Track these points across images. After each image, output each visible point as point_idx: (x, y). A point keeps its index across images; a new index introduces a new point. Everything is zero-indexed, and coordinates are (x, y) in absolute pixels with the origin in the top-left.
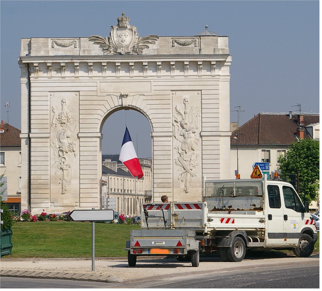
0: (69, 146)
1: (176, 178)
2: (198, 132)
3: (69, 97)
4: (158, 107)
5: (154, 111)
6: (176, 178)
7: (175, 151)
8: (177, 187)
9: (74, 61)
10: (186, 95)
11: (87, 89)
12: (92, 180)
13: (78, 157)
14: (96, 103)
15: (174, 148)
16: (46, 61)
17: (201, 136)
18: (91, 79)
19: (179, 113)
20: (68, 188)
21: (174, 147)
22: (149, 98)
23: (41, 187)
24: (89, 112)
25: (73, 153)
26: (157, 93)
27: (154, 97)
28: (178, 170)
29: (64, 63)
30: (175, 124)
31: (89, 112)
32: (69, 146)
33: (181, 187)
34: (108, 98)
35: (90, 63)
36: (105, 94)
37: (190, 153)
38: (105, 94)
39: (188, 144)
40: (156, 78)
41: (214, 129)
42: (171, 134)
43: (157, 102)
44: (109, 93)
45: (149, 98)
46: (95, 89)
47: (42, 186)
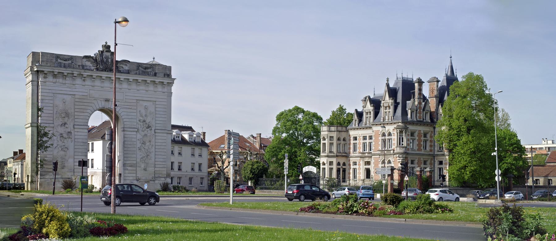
0: (68, 134)
1: (138, 160)
2: (153, 129)
3: (68, 98)
4: (129, 110)
5: (125, 113)
6: (138, 160)
7: (138, 142)
9: (74, 72)
10: (145, 104)
11: (81, 94)
13: (73, 142)
14: (86, 104)
16: (54, 71)
17: (155, 132)
18: (84, 87)
19: (141, 116)
20: (66, 165)
22: (123, 104)
24: (82, 110)
25: (70, 139)
27: (126, 104)
28: (140, 155)
29: (66, 73)
30: (139, 123)
31: (82, 110)
32: (68, 134)
33: (142, 167)
34: (95, 102)
35: (85, 75)
36: (93, 99)
37: (148, 144)
38: (93, 99)
40: (127, 90)
41: (163, 128)
42: (136, 130)
45: (123, 104)
46: (86, 94)
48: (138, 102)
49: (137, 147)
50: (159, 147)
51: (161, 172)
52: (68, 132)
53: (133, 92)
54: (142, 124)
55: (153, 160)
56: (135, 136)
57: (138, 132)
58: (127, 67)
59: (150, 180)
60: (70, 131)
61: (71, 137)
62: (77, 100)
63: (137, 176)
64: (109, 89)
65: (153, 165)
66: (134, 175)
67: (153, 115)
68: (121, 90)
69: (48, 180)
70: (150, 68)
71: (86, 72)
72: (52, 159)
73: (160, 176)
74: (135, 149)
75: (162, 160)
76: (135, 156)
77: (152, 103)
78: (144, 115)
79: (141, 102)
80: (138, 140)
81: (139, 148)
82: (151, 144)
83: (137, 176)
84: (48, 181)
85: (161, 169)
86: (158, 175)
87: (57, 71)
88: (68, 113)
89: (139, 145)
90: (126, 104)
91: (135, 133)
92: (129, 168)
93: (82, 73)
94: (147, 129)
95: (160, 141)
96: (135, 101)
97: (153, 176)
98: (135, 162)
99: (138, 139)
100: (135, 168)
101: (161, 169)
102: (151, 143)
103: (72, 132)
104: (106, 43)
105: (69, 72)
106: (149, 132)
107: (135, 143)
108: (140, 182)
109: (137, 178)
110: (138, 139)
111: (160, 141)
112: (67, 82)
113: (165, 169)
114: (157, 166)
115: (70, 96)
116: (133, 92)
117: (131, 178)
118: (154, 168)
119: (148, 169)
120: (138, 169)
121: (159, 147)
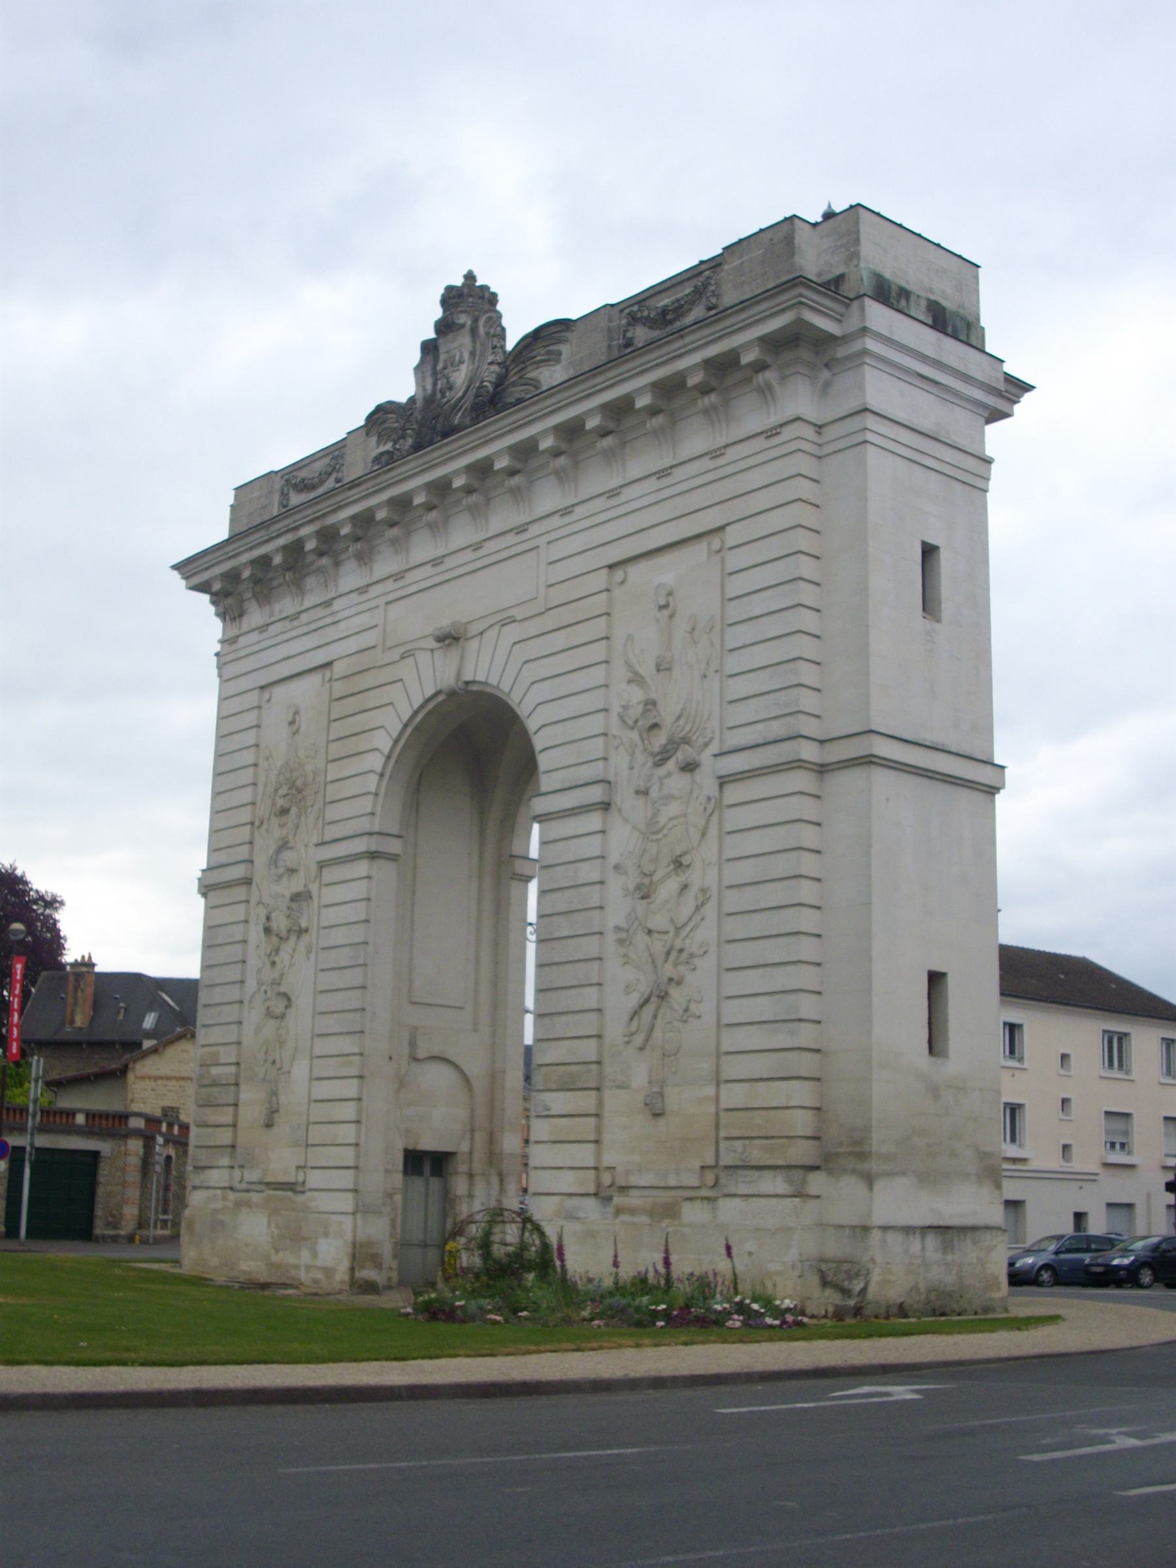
1: (615, 1030)
6: (615, 1030)
8: (619, 1087)
11: (351, 645)
18: (364, 597)
22: (533, 627)
26: (559, 595)
27: (548, 621)
29: (277, 550)
34: (405, 670)
35: (343, 522)
37: (668, 888)
38: (396, 654)
39: (660, 836)
42: (595, 794)
43: (559, 640)
44: (408, 647)
45: (533, 627)
48: (619, 575)
49: (611, 924)
51: (758, 1118)
52: (296, 897)
54: (634, 735)
55: (709, 1020)
56: (592, 846)
57: (613, 811)
58: (558, 367)
59: (687, 1199)
60: (301, 888)
61: (304, 924)
62: (339, 689)
64: (469, 555)
65: (706, 1066)
66: (584, 1155)
67: (712, 644)
68: (527, 535)
71: (340, 508)
72: (233, 1069)
73: (756, 1155)
74: (590, 947)
75: (765, 1008)
76: (590, 997)
77: (700, 550)
78: (646, 669)
79: (634, 571)
80: (617, 867)
81: (618, 929)
82: (685, 887)
83: (608, 1159)
86: (739, 1144)
87: (245, 558)
88: (299, 783)
89: (618, 910)
91: (593, 821)
92: (558, 1102)
94: (662, 771)
96: (599, 580)
97: (710, 1161)
98: (589, 1050)
99: (614, 857)
100: (587, 1101)
102: (695, 877)
103: (314, 888)
104: (470, 277)
105: (282, 541)
106: (678, 783)
107: (593, 896)
108: (618, 1211)
109: (606, 1179)
110: (614, 857)
112: (310, 601)
113: (801, 1093)
116: (587, 523)
117: (567, 1182)
118: (710, 1091)
119: (675, 1098)
120: (613, 1100)
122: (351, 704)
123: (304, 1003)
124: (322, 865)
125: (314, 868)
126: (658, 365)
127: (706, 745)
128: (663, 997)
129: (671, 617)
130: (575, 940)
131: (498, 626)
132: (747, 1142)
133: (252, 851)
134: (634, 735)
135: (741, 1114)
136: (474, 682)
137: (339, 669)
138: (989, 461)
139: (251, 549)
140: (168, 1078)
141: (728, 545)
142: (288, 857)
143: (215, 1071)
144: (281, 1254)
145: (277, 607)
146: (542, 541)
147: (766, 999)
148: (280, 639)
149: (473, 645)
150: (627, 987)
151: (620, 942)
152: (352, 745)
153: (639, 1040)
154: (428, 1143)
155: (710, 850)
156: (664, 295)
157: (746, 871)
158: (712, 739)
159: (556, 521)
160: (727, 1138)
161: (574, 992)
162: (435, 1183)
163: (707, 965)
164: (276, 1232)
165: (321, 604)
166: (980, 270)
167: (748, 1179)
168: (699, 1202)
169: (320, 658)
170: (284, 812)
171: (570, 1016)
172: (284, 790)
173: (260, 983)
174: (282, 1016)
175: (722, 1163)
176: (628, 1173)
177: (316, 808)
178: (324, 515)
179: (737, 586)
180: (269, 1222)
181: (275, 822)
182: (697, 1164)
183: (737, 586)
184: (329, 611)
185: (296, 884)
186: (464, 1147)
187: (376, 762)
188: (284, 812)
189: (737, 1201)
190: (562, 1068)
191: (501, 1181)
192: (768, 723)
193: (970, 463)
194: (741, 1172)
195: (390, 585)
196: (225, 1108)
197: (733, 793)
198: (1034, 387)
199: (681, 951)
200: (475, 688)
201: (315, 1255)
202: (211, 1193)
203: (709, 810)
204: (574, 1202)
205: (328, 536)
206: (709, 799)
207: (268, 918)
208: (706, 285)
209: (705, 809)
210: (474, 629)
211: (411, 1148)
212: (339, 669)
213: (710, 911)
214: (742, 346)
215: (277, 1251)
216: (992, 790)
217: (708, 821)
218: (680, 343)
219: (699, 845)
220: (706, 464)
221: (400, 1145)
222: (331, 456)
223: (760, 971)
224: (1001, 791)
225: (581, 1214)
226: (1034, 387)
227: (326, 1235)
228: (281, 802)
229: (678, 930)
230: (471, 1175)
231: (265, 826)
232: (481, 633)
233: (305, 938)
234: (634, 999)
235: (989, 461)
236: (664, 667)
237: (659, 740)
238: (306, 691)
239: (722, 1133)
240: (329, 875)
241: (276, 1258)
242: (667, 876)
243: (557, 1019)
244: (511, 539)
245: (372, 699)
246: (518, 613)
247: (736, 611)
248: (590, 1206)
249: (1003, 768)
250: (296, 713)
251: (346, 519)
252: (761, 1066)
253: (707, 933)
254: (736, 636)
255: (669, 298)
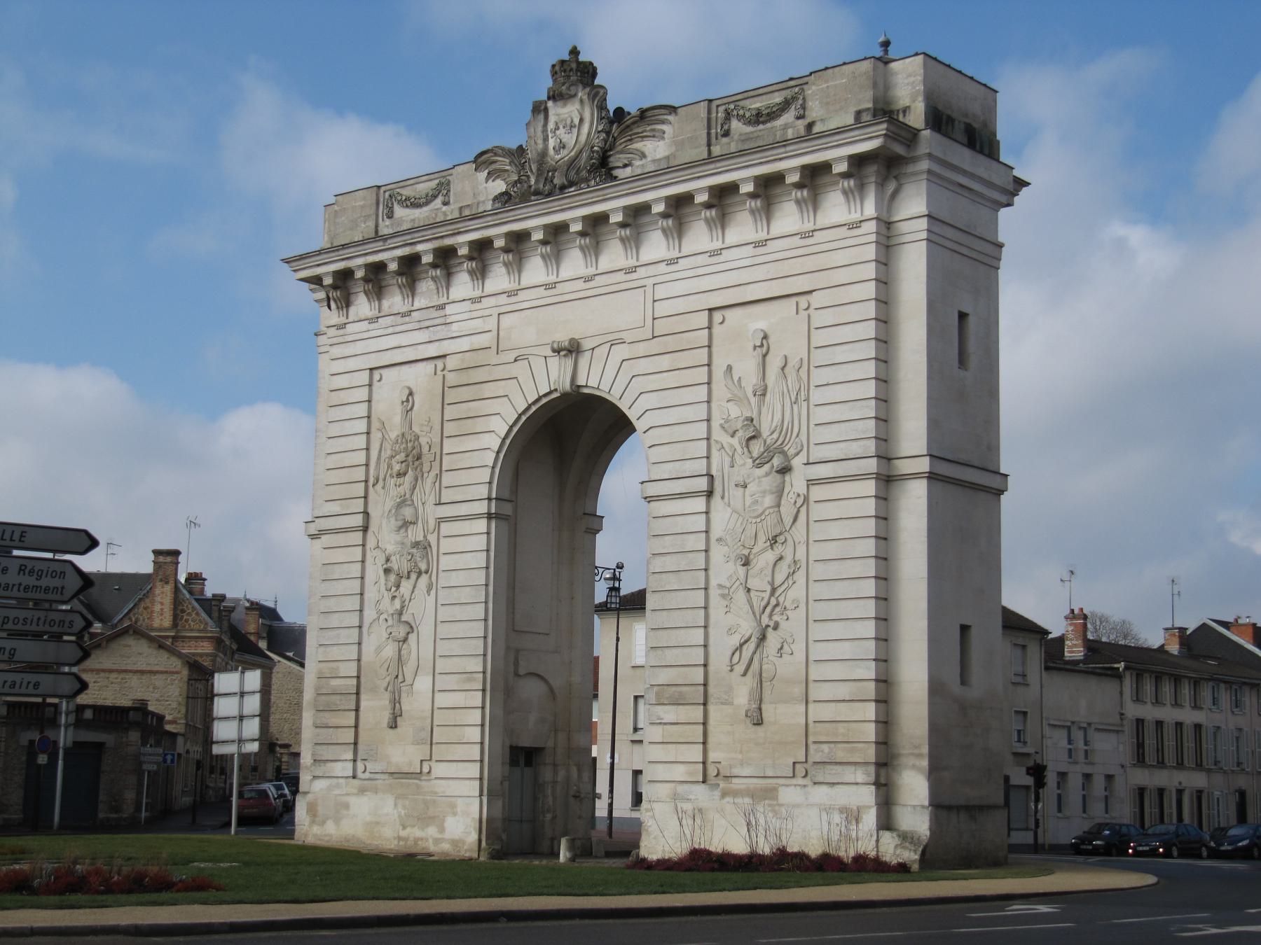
6: (719, 660)
8: (722, 703)
10: (758, 320)
11: (464, 344)
12: (468, 675)
15: (717, 540)
18: (477, 306)
21: (718, 536)
22: (642, 349)
23: (338, 703)
29: (393, 259)
33: (735, 703)
34: (520, 369)
43: (665, 362)
45: (642, 349)
47: (341, 700)
50: (832, 570)
51: (841, 728)
53: (690, 273)
54: (735, 442)
55: (800, 656)
58: (661, 143)
62: (452, 379)
63: (712, 756)
64: (580, 284)
65: (798, 690)
69: (338, 786)
70: (785, 106)
73: (840, 755)
77: (789, 305)
79: (730, 314)
80: (719, 540)
81: (720, 586)
82: (781, 558)
84: (337, 792)
85: (844, 712)
86: (825, 747)
87: (360, 261)
90: (655, 346)
93: (448, 242)
95: (835, 530)
101: (844, 712)
103: (432, 539)
104: (575, 52)
105: (400, 252)
111: (835, 530)
114: (816, 692)
115: (428, 367)
116: (690, 273)
117: (679, 772)
121: (832, 570)
122: (465, 393)
123: (426, 630)
124: (440, 520)
125: (432, 523)
126: (761, 163)
127: (797, 454)
128: (763, 638)
129: (765, 356)
130: (683, 593)
131: (609, 344)
132: (832, 745)
133: (366, 504)
134: (735, 442)
135: (827, 725)
136: (586, 386)
137: (452, 363)
138: (1001, 246)
139: (366, 254)
140: (111, 671)
141: (814, 305)
142: (408, 512)
143: (334, 682)
144: (408, 830)
145: (386, 303)
146: (650, 282)
147: (846, 644)
148: (390, 330)
149: (588, 354)
150: (730, 629)
151: (723, 596)
152: (469, 426)
153: (740, 669)
154: (526, 742)
155: (799, 531)
156: (756, 99)
157: (831, 550)
158: (801, 450)
159: (662, 268)
160: (815, 742)
161: (683, 631)
162: (527, 770)
163: (798, 616)
164: (403, 812)
165: (433, 307)
166: (998, 94)
167: (834, 771)
168: (793, 787)
169: (432, 350)
170: (401, 475)
171: (680, 650)
172: (401, 457)
173: (380, 613)
174: (405, 640)
175: (811, 760)
176: (731, 767)
177: (433, 474)
178: (442, 237)
179: (819, 338)
180: (396, 805)
181: (392, 482)
182: (791, 761)
183: (819, 338)
184: (441, 313)
185: (416, 534)
186: (550, 744)
187: (495, 443)
188: (401, 475)
189: (824, 788)
190: (674, 689)
191: (579, 770)
192: (848, 443)
193: (989, 249)
194: (829, 767)
195: (503, 299)
196: (347, 713)
197: (817, 493)
198: (1029, 184)
199: (777, 605)
200: (586, 391)
201: (442, 829)
202: (334, 781)
203: (798, 505)
204: (686, 787)
205: (445, 257)
206: (799, 495)
207: (388, 560)
208: (794, 98)
209: (796, 502)
210: (587, 345)
211: (514, 745)
212: (452, 363)
213: (800, 577)
214: (835, 159)
215: (404, 828)
216: (1000, 492)
217: (798, 511)
218: (782, 150)
219: (790, 528)
220: (796, 241)
221: (508, 744)
222: (437, 181)
223: (843, 623)
224: (1005, 492)
225: (692, 797)
226: (1029, 184)
227: (455, 814)
228: (397, 467)
229: (774, 590)
230: (555, 765)
231: (381, 483)
232: (593, 349)
233: (424, 579)
234: (735, 640)
235: (1001, 246)
236: (762, 393)
237: (757, 448)
238: (418, 376)
239: (811, 739)
240: (446, 528)
241: (403, 833)
242: (765, 550)
243: (667, 651)
244: (620, 277)
245: (488, 390)
246: (627, 336)
247: (820, 357)
248: (700, 792)
249: (1007, 476)
250: (411, 394)
251: (464, 243)
252: (843, 691)
253: (796, 592)
254: (819, 376)
255: (761, 102)
